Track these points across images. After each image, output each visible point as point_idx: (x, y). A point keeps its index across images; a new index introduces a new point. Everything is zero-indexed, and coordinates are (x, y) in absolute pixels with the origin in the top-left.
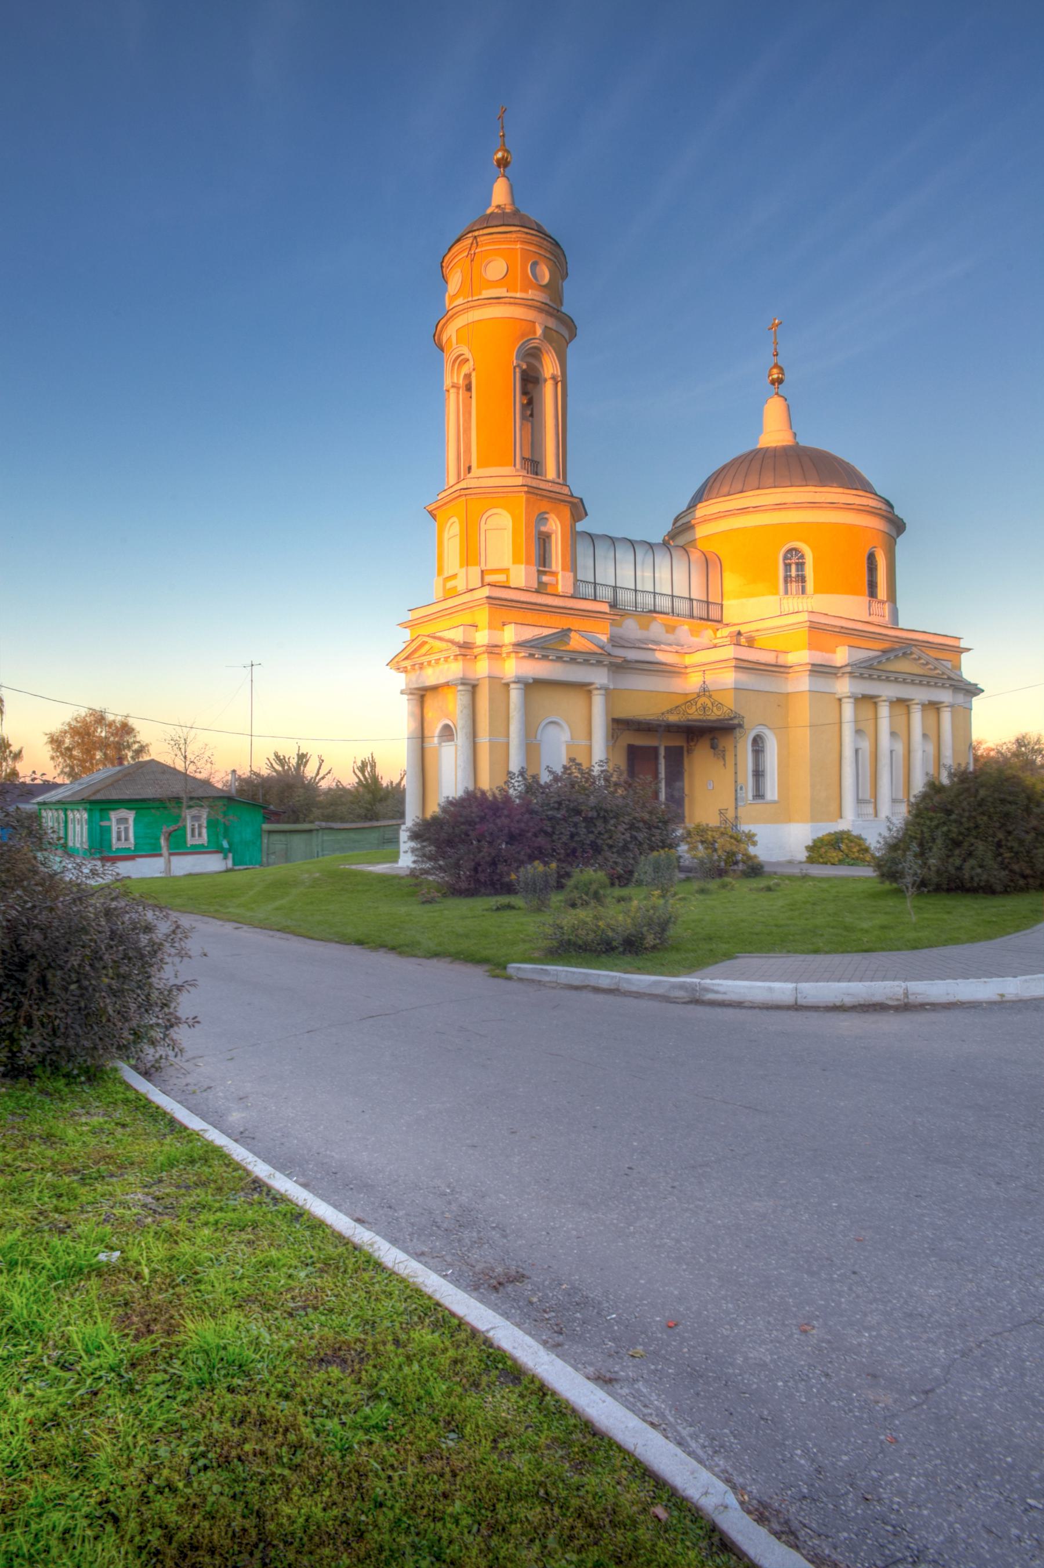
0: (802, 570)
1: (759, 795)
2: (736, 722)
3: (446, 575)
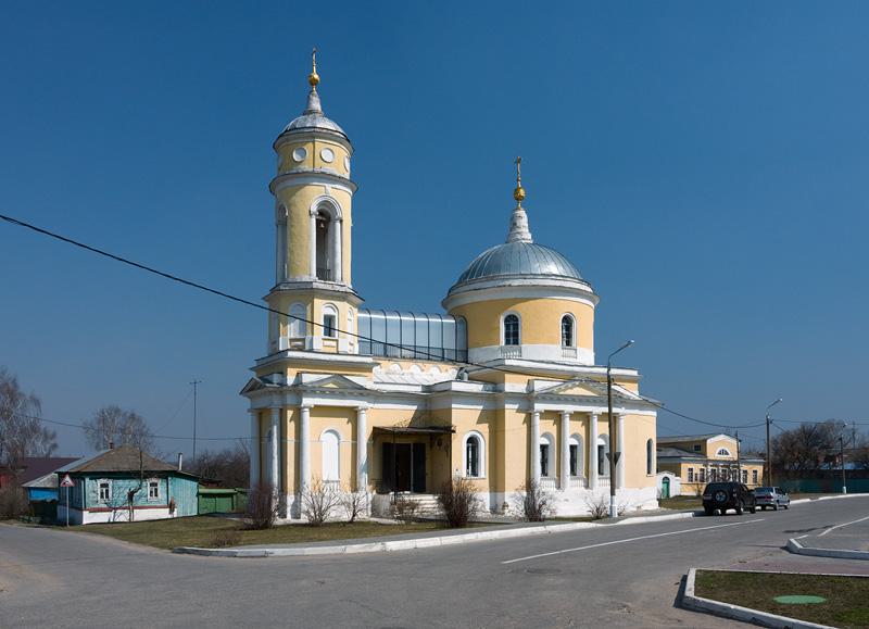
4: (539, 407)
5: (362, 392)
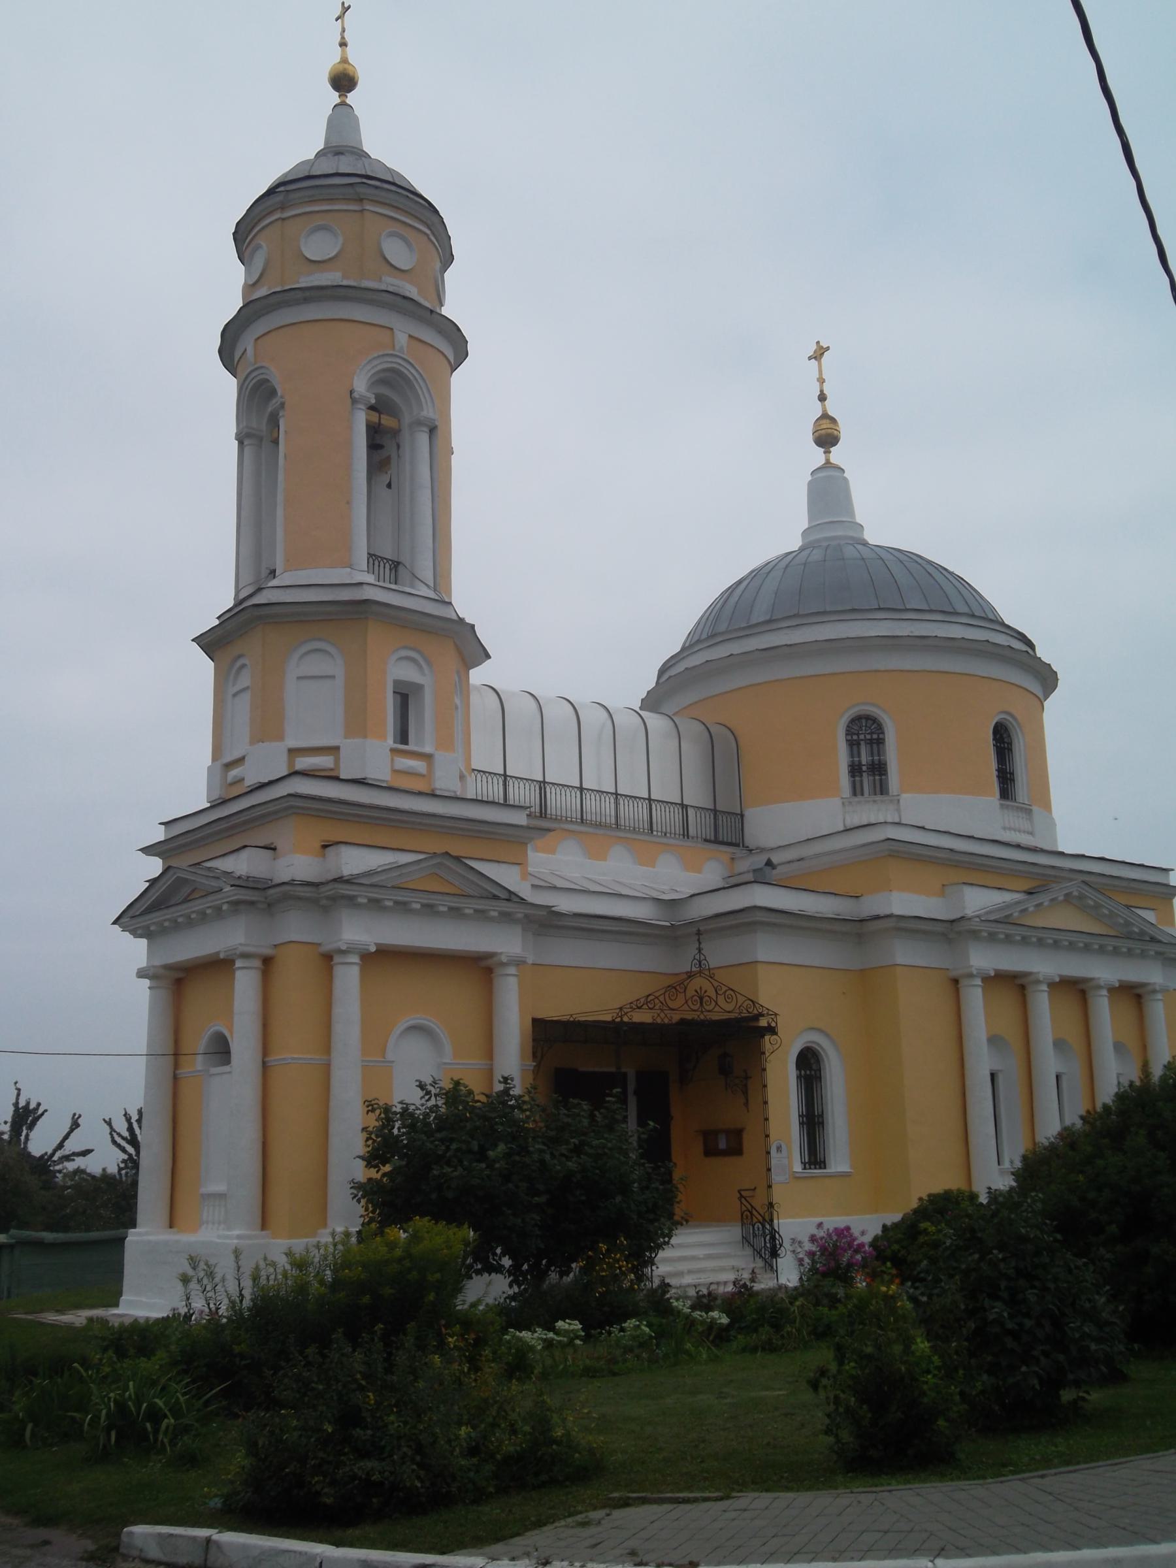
1: (815, 1157)
2: (763, 1023)
3: (228, 758)
4: (983, 959)
5: (504, 905)
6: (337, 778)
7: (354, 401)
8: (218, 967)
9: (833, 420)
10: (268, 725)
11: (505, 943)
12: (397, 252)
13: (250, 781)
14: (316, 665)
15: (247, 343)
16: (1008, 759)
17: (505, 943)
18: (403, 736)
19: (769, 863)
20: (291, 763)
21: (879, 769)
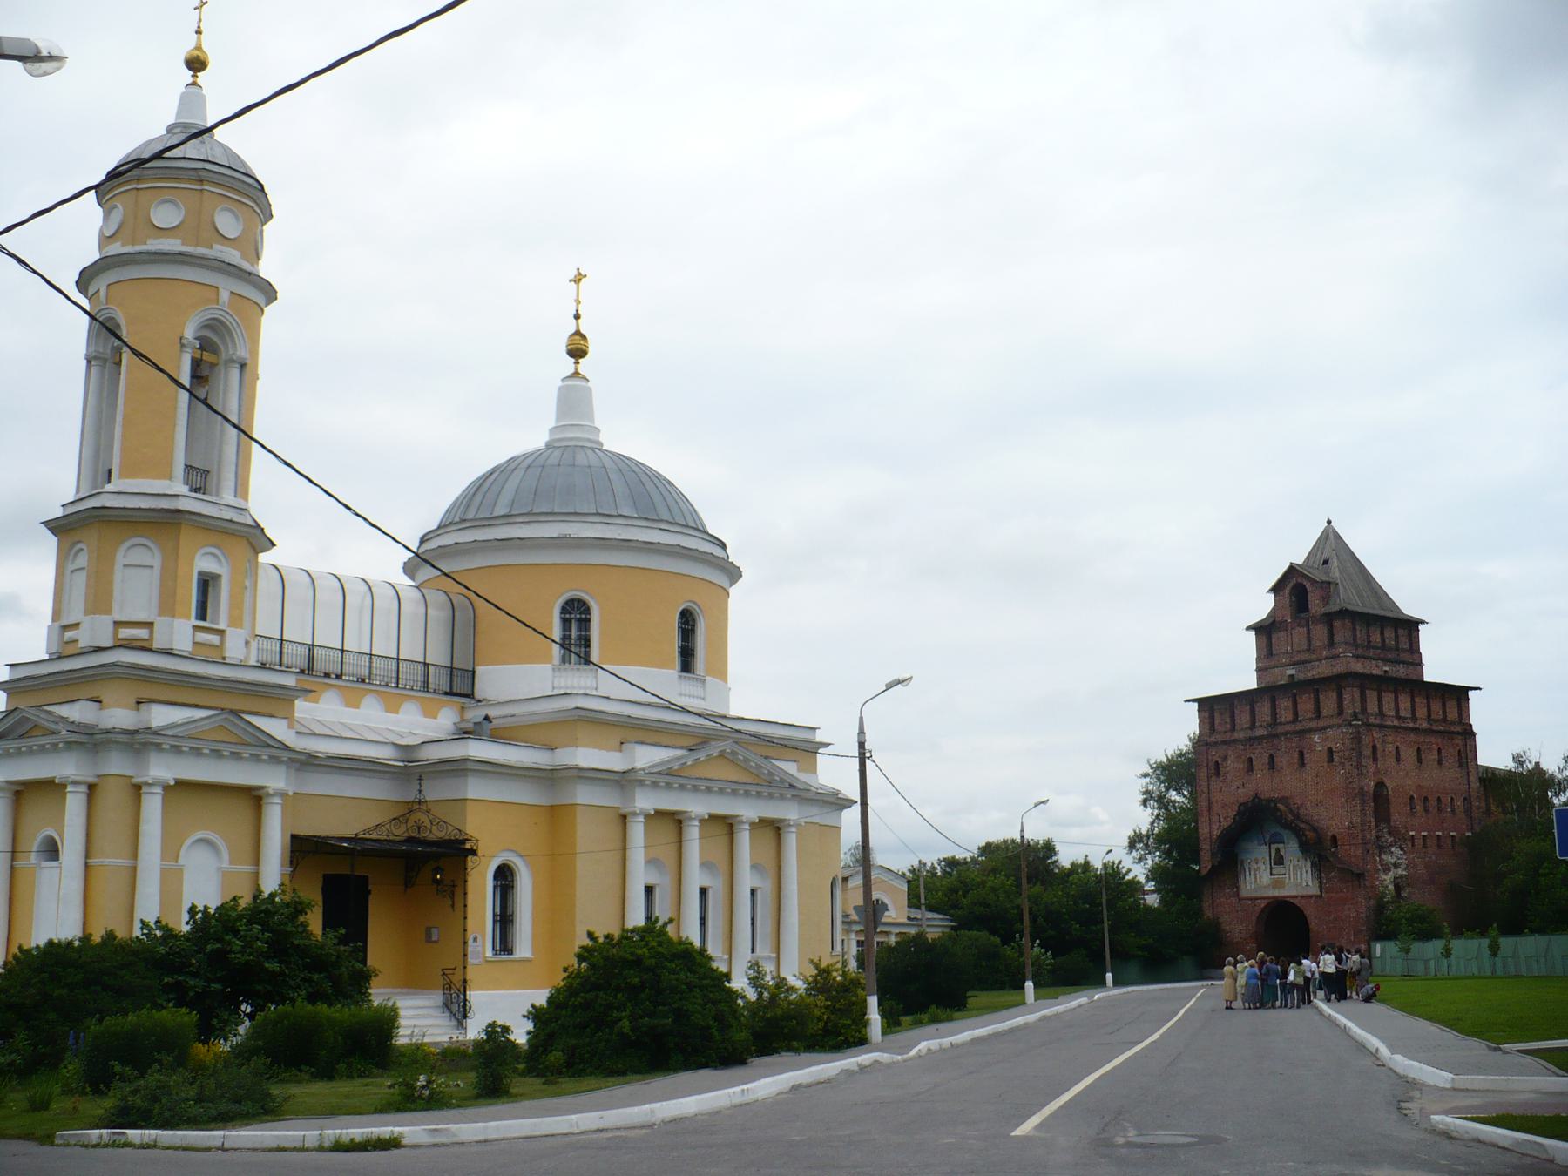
0: (588, 629)
2: (468, 846)
4: (646, 801)
6: (150, 650)
7: (183, 346)
8: (52, 788)
9: (584, 337)
10: (99, 601)
11: (274, 780)
12: (228, 224)
13: (82, 644)
14: (140, 556)
15: (100, 285)
16: (690, 643)
17: (274, 780)
18: (202, 615)
19: (487, 718)
20: (115, 633)
21: (586, 642)
